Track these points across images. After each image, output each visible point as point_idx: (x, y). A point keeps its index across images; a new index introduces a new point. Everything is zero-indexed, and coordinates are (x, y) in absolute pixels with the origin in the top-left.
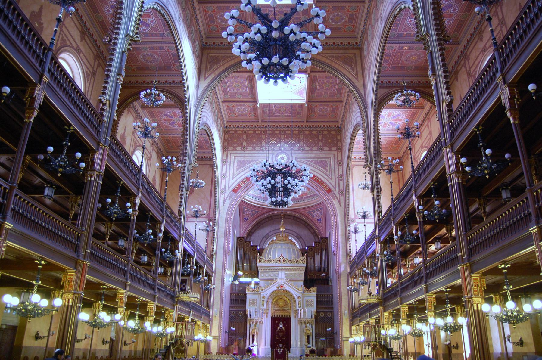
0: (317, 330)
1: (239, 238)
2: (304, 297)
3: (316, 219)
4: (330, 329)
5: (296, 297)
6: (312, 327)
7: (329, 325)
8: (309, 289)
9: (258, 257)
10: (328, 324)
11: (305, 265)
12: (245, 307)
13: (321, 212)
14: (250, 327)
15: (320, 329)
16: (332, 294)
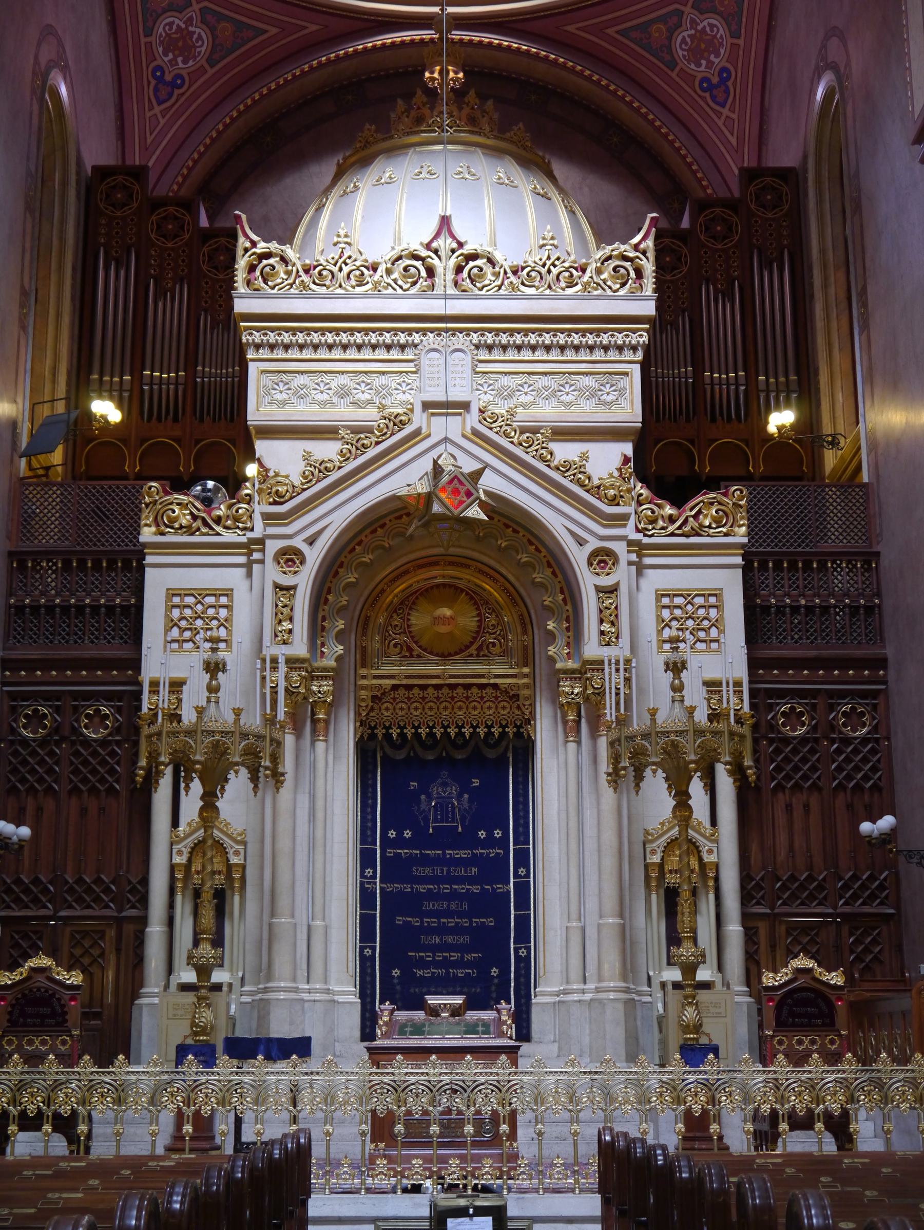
0: (754, 848)
1: (101, 172)
2: (641, 569)
3: (688, 77)
4: (887, 822)
5: (578, 557)
6: (714, 822)
7: (850, 806)
8: (678, 503)
9: (242, 242)
10: (841, 800)
11: (648, 308)
12: (136, 664)
13: (732, 19)
14: (175, 823)
15: (782, 839)
16: (870, 558)
